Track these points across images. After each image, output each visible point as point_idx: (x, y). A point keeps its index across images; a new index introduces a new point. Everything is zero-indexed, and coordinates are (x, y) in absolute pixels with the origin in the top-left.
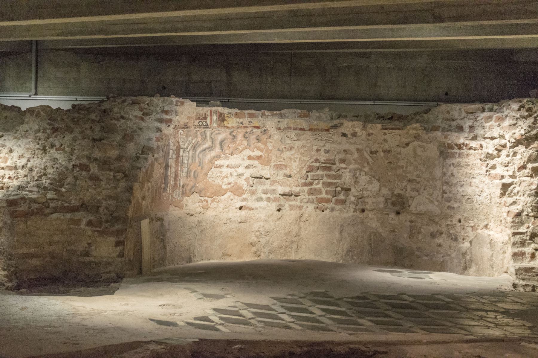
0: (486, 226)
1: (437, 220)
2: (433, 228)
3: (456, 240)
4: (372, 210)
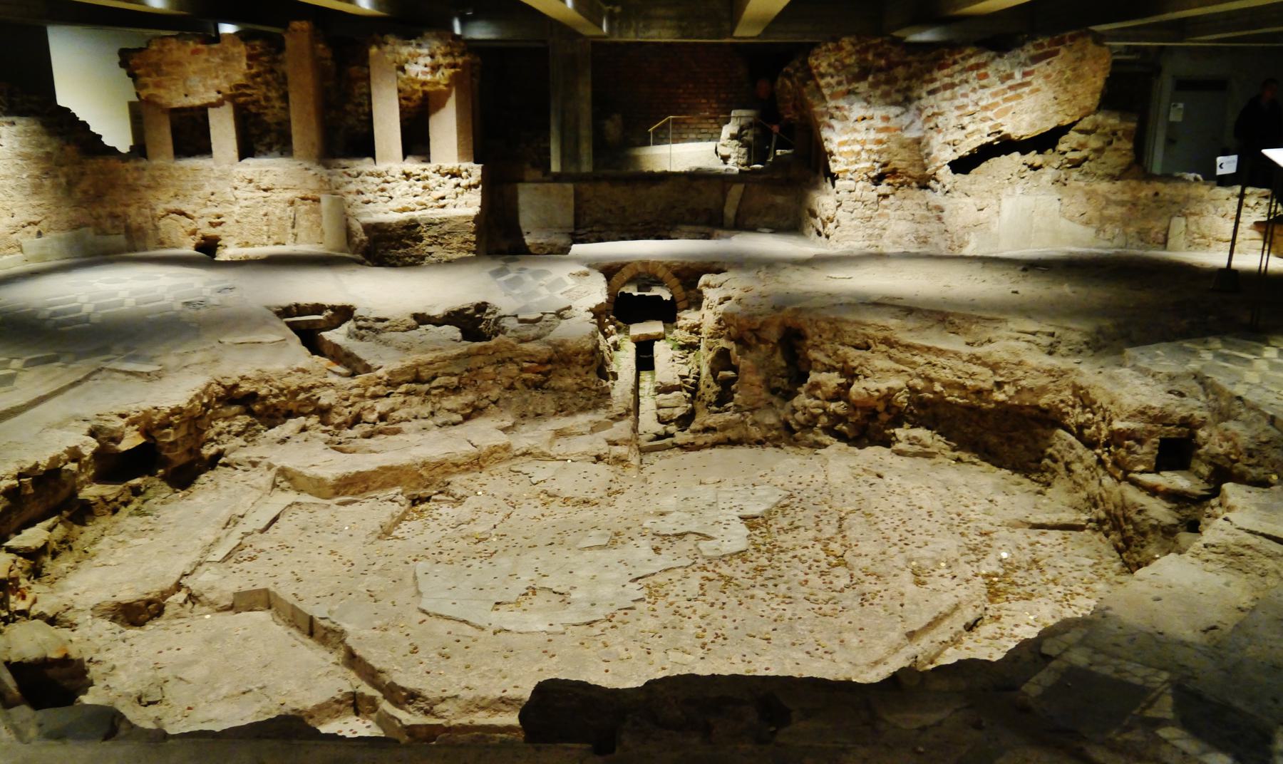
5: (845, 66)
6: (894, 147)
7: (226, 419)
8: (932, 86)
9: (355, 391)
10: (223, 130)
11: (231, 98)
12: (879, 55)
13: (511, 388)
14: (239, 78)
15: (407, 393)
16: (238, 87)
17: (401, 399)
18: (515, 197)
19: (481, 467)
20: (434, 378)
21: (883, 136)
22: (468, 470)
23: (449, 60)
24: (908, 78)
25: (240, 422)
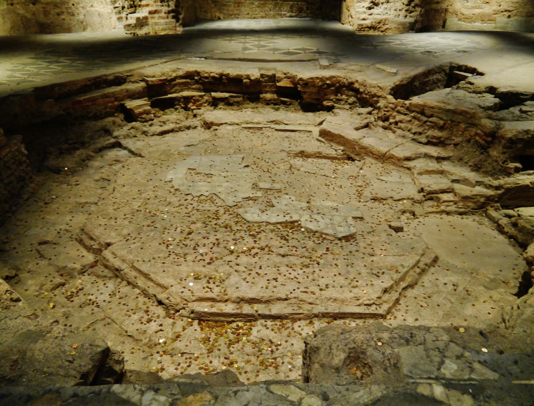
0: (92, 6)
1: (59, 5)
2: (58, 10)
3: (73, 15)
4: (18, 4)
7: (347, 96)
9: (391, 105)
13: (469, 141)
15: (414, 117)
17: (409, 119)
19: (384, 162)
20: (432, 116)
22: (377, 159)
25: (352, 100)
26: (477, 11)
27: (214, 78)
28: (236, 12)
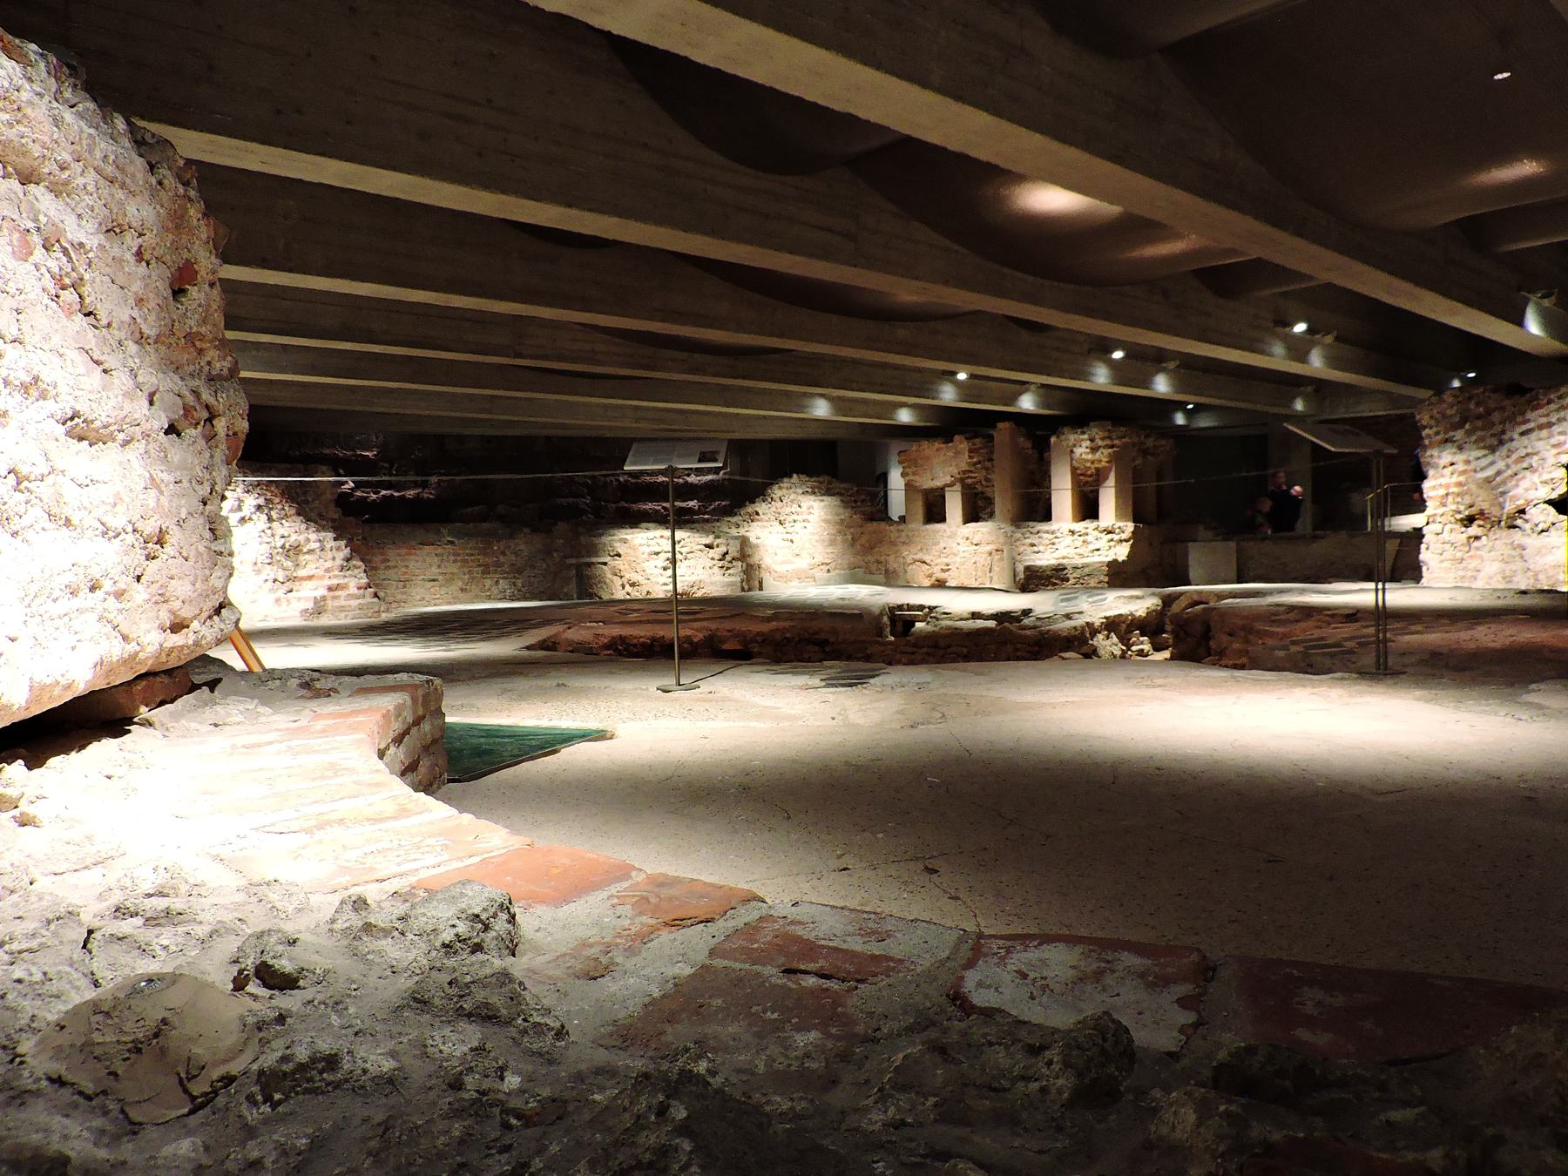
5: (1444, 416)
6: (1473, 487)
8: (1524, 428)
10: (954, 506)
11: (962, 481)
12: (1478, 404)
14: (964, 467)
16: (964, 472)
18: (1186, 555)
21: (1462, 479)
23: (1108, 442)
24: (1503, 422)
26: (789, 567)
27: (643, 644)
28: (400, 597)
